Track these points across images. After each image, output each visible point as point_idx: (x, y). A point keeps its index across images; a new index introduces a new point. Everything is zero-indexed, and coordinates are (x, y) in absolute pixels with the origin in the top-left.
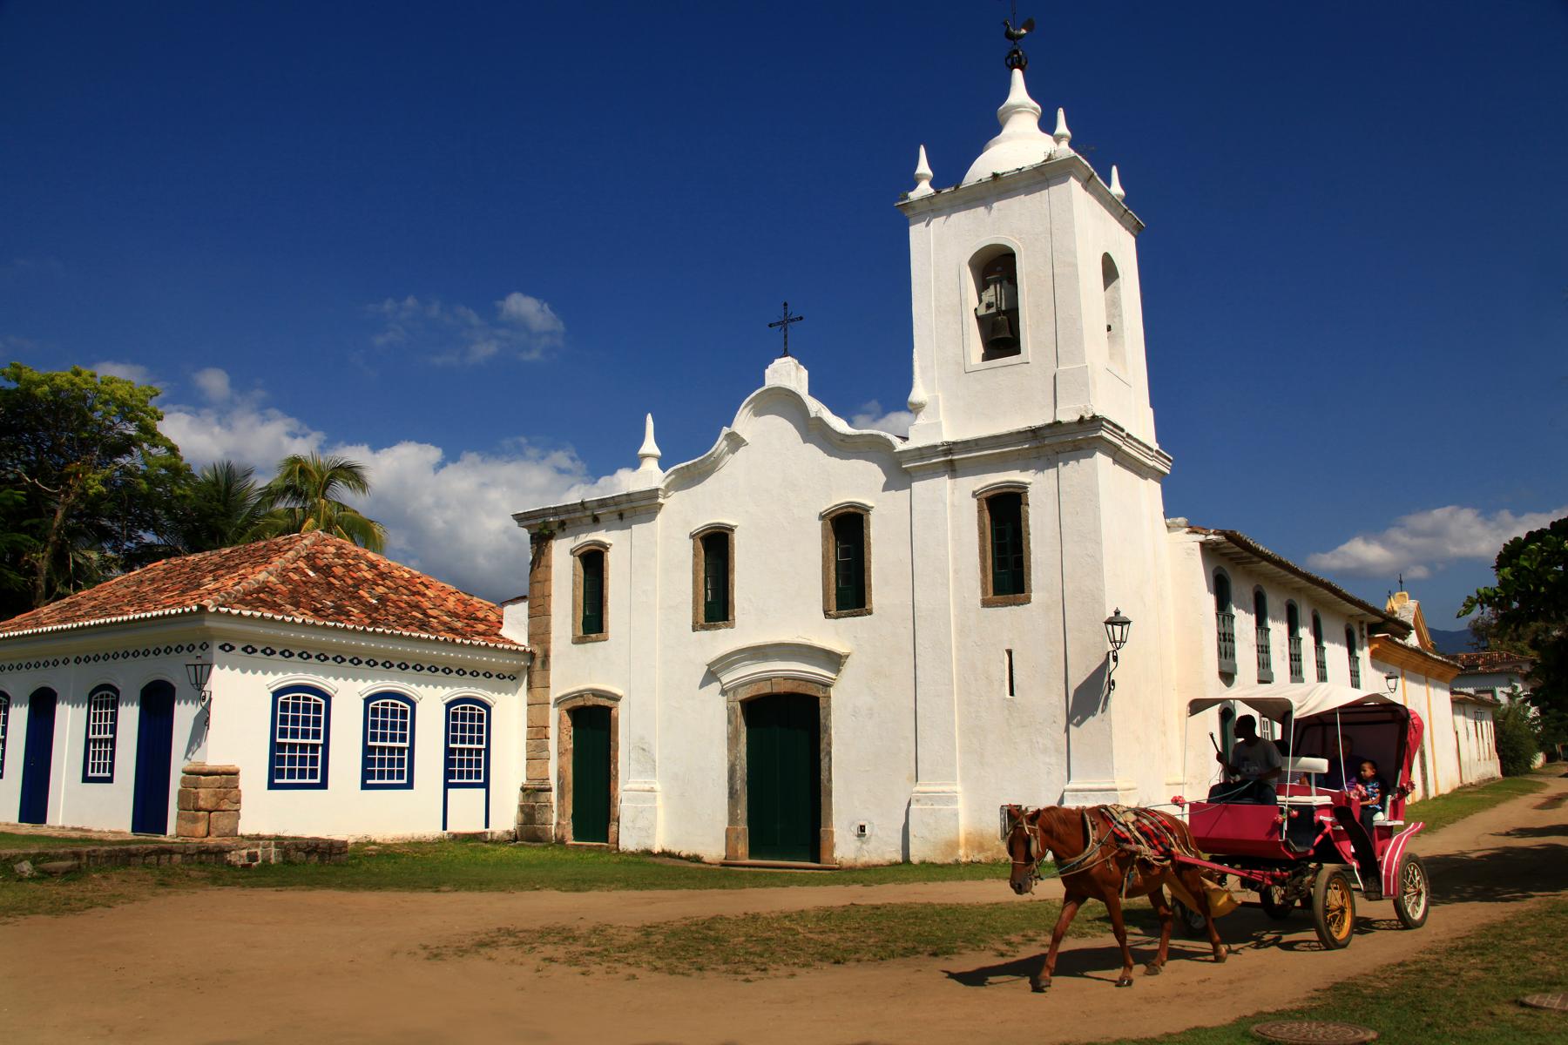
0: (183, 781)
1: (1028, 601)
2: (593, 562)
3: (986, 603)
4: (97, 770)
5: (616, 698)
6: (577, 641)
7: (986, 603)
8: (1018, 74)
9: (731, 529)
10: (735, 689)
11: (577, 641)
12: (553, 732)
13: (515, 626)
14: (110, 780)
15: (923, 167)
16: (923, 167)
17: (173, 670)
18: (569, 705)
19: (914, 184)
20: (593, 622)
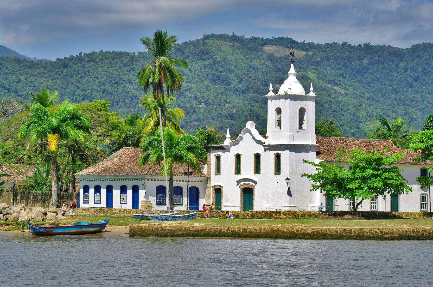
0: (142, 203)
1: (280, 174)
2: (218, 158)
3: (275, 174)
4: (123, 201)
5: (222, 187)
6: (216, 175)
7: (275, 174)
8: (292, 65)
9: (241, 155)
10: (241, 186)
11: (216, 175)
12: (211, 194)
13: (205, 171)
14: (126, 204)
15: (271, 88)
16: (271, 88)
17: (139, 183)
18: (214, 188)
19: (269, 91)
20: (218, 171)
